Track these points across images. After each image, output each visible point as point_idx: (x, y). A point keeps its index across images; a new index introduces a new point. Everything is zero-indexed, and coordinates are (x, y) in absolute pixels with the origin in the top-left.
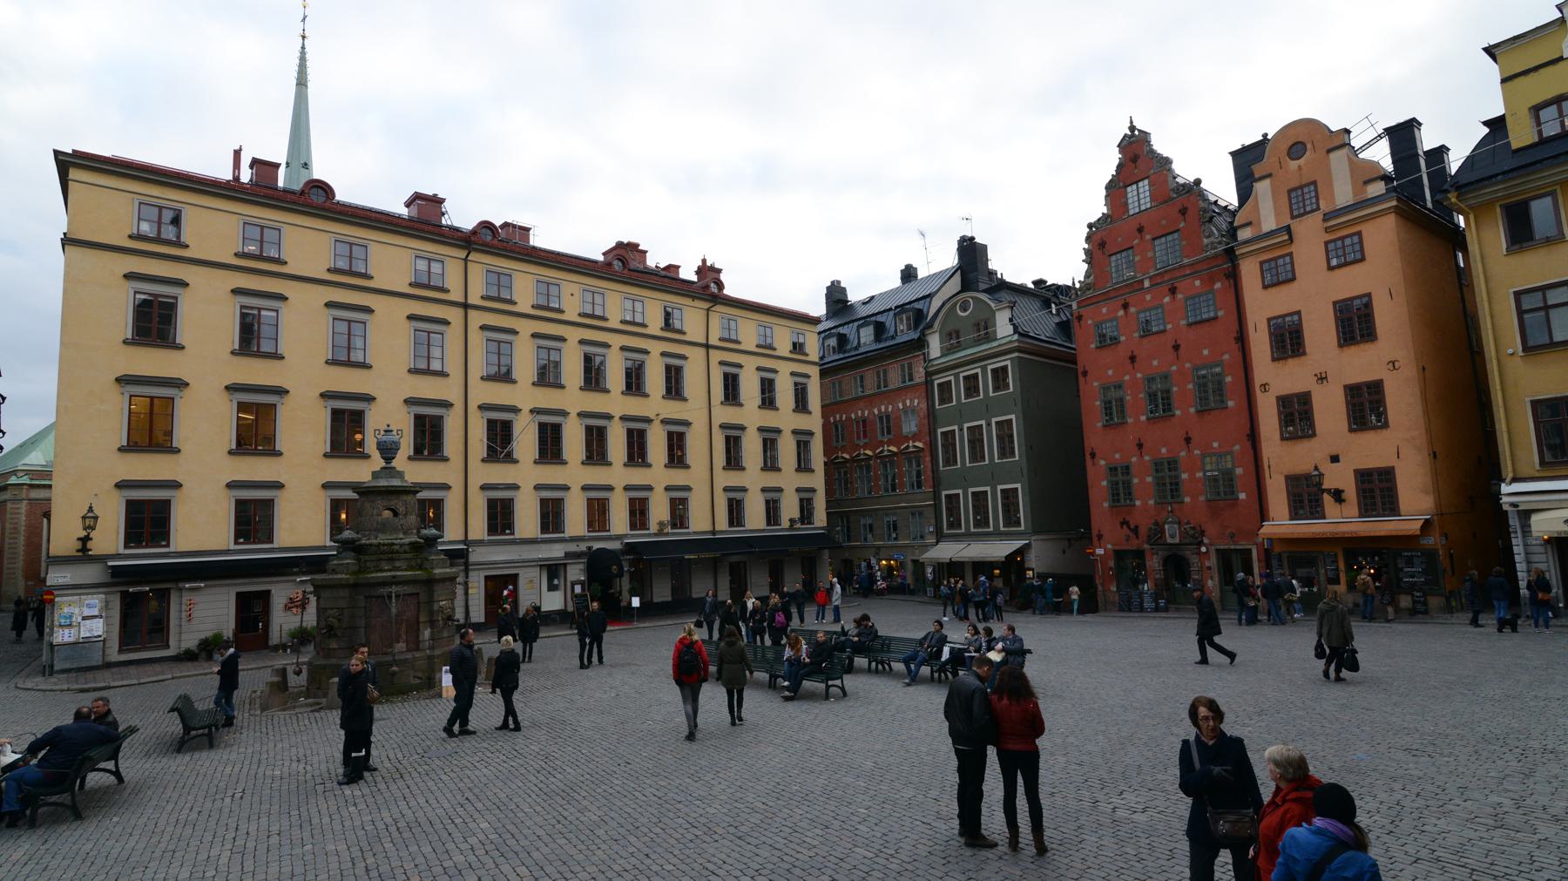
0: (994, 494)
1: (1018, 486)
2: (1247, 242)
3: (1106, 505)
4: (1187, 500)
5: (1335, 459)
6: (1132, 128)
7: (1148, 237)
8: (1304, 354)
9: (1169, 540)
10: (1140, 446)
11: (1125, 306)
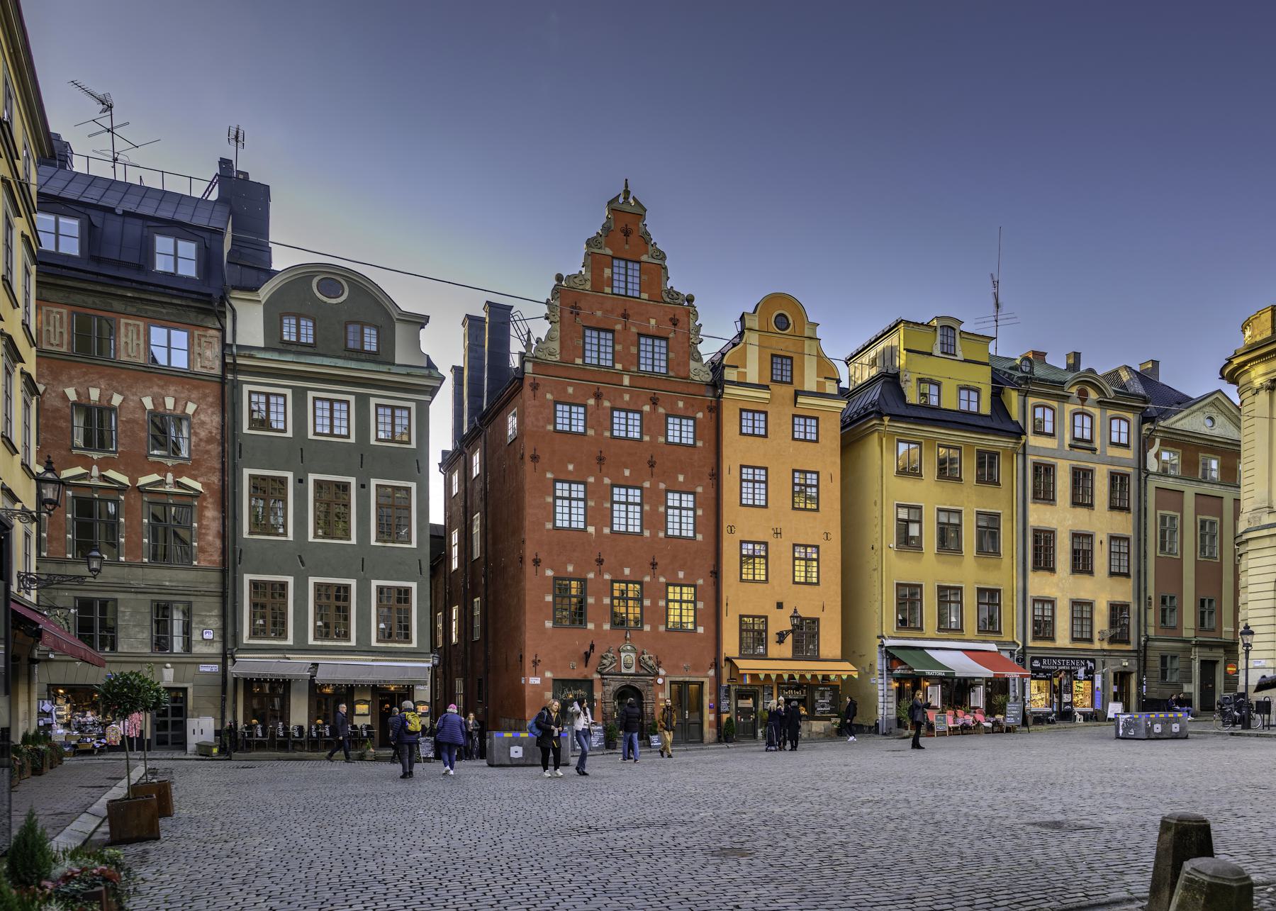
2: (732, 383)
7: (634, 330)
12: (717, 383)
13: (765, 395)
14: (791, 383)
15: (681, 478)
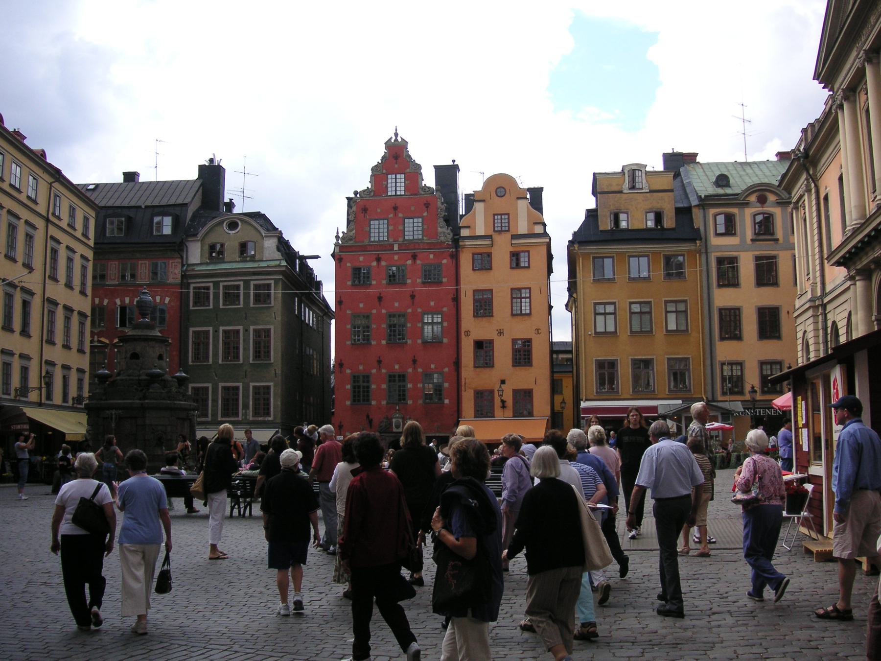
0: (245, 389)
1: (271, 384)
3: (348, 403)
4: (410, 402)
5: (503, 382)
6: (396, 135)
8: (492, 316)
9: (395, 430)
10: (379, 362)
11: (378, 260)
12: (457, 240)
13: (487, 242)
14: (508, 231)
15: (432, 304)
